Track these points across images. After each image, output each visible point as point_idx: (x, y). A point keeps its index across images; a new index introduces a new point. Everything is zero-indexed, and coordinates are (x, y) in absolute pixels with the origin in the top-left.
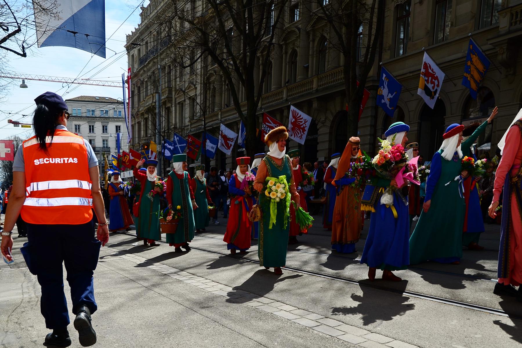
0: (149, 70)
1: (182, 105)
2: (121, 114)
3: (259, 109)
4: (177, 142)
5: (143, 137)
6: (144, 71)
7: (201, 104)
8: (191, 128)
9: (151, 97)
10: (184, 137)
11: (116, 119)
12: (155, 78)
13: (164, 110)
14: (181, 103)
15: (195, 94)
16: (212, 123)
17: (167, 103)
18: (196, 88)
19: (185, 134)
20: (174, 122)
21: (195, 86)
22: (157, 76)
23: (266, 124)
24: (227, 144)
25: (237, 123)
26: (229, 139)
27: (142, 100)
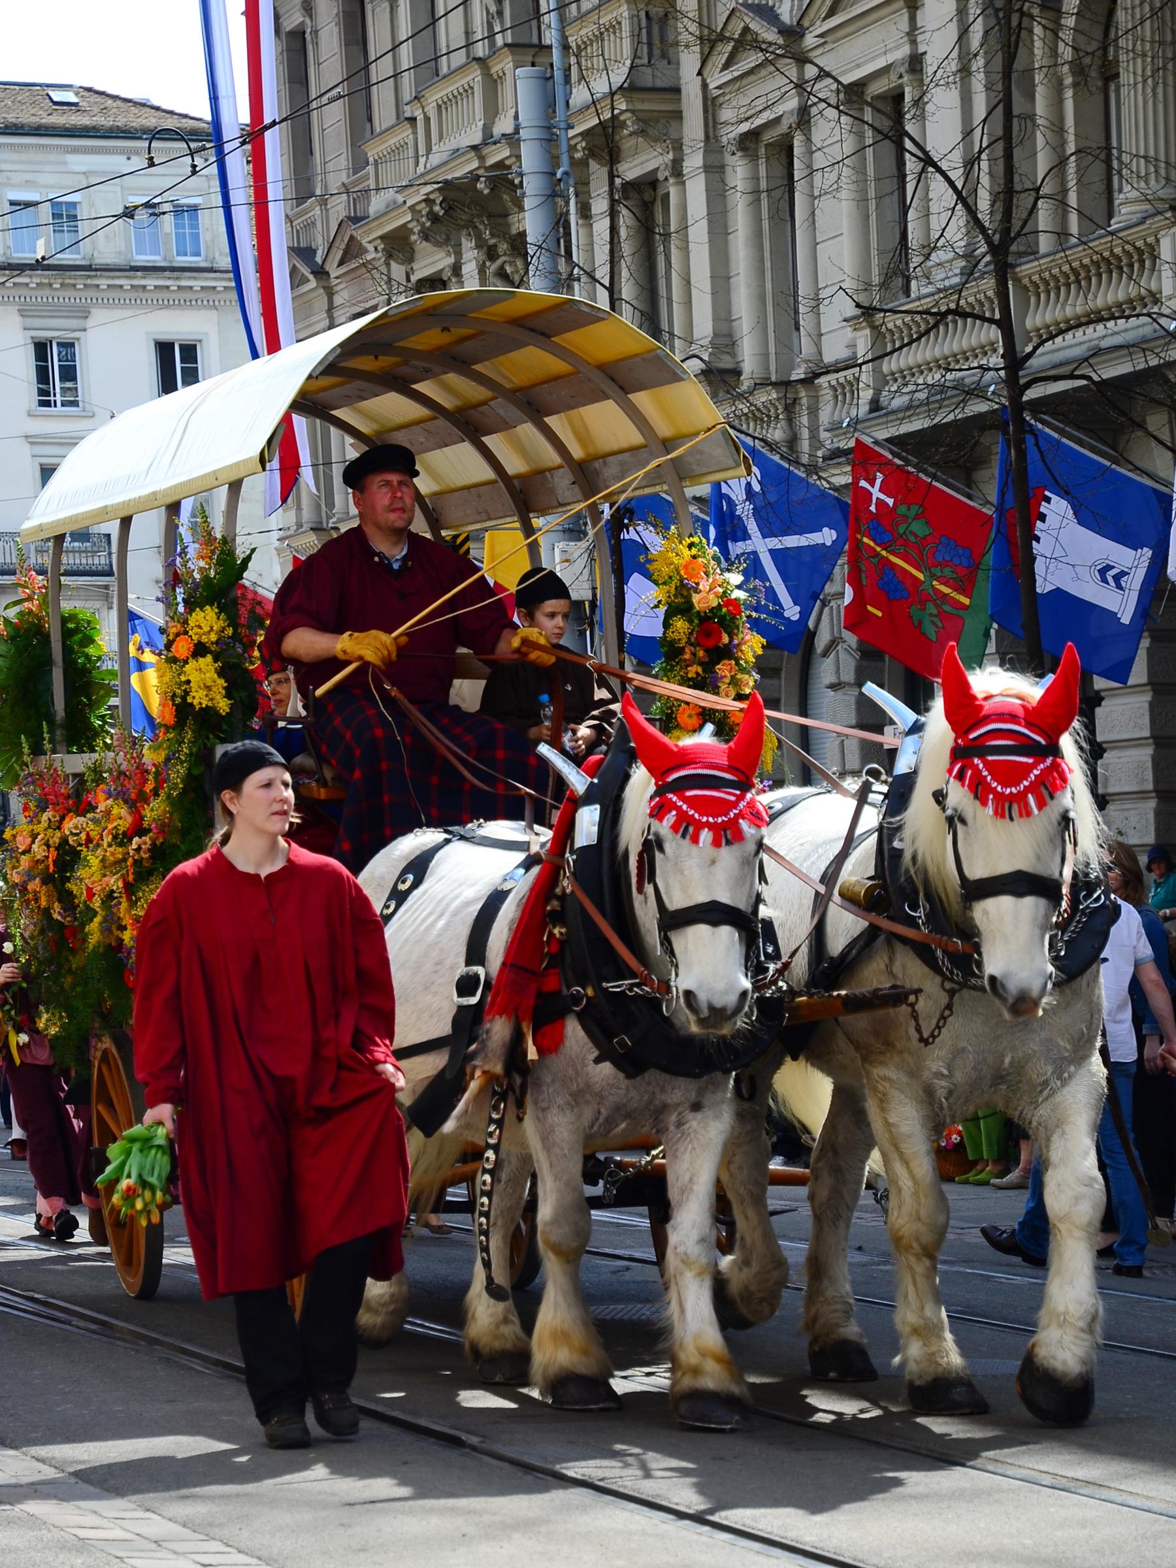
2: (196, 237)
4: (744, 510)
7: (970, 163)
8: (882, 381)
9: (468, 90)
10: (812, 469)
11: (151, 282)
13: (600, 206)
14: (769, 136)
15: (906, 50)
17: (627, 145)
19: (824, 435)
20: (704, 327)
27: (384, 114)
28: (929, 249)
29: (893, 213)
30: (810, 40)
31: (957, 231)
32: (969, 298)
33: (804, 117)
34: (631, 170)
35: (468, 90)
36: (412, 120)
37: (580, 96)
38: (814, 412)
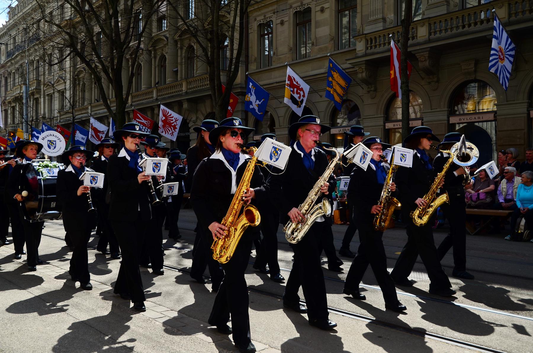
0: (16, 63)
1: (51, 96)
3: (129, 106)
5: (10, 124)
6: (12, 63)
7: (70, 98)
8: (60, 119)
9: (18, 88)
10: (53, 127)
12: (23, 71)
13: (32, 100)
14: (50, 95)
16: (82, 115)
17: (35, 94)
18: (65, 83)
19: (55, 124)
20: (42, 112)
21: (64, 80)
22: (25, 68)
23: (136, 120)
24: (98, 136)
25: (107, 117)
26: (100, 132)
27: (9, 89)
28: (66, 106)
29: (62, 102)
30: (55, 85)
31: (68, 105)
32: (69, 111)
33: (54, 93)
34: (35, 97)
35: (18, 88)
36: (12, 90)
37: (30, 89)
38: (53, 121)
